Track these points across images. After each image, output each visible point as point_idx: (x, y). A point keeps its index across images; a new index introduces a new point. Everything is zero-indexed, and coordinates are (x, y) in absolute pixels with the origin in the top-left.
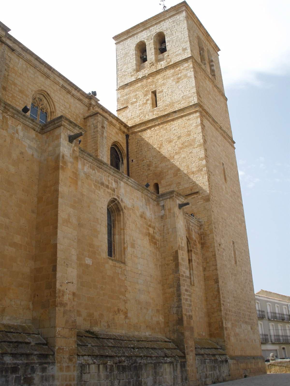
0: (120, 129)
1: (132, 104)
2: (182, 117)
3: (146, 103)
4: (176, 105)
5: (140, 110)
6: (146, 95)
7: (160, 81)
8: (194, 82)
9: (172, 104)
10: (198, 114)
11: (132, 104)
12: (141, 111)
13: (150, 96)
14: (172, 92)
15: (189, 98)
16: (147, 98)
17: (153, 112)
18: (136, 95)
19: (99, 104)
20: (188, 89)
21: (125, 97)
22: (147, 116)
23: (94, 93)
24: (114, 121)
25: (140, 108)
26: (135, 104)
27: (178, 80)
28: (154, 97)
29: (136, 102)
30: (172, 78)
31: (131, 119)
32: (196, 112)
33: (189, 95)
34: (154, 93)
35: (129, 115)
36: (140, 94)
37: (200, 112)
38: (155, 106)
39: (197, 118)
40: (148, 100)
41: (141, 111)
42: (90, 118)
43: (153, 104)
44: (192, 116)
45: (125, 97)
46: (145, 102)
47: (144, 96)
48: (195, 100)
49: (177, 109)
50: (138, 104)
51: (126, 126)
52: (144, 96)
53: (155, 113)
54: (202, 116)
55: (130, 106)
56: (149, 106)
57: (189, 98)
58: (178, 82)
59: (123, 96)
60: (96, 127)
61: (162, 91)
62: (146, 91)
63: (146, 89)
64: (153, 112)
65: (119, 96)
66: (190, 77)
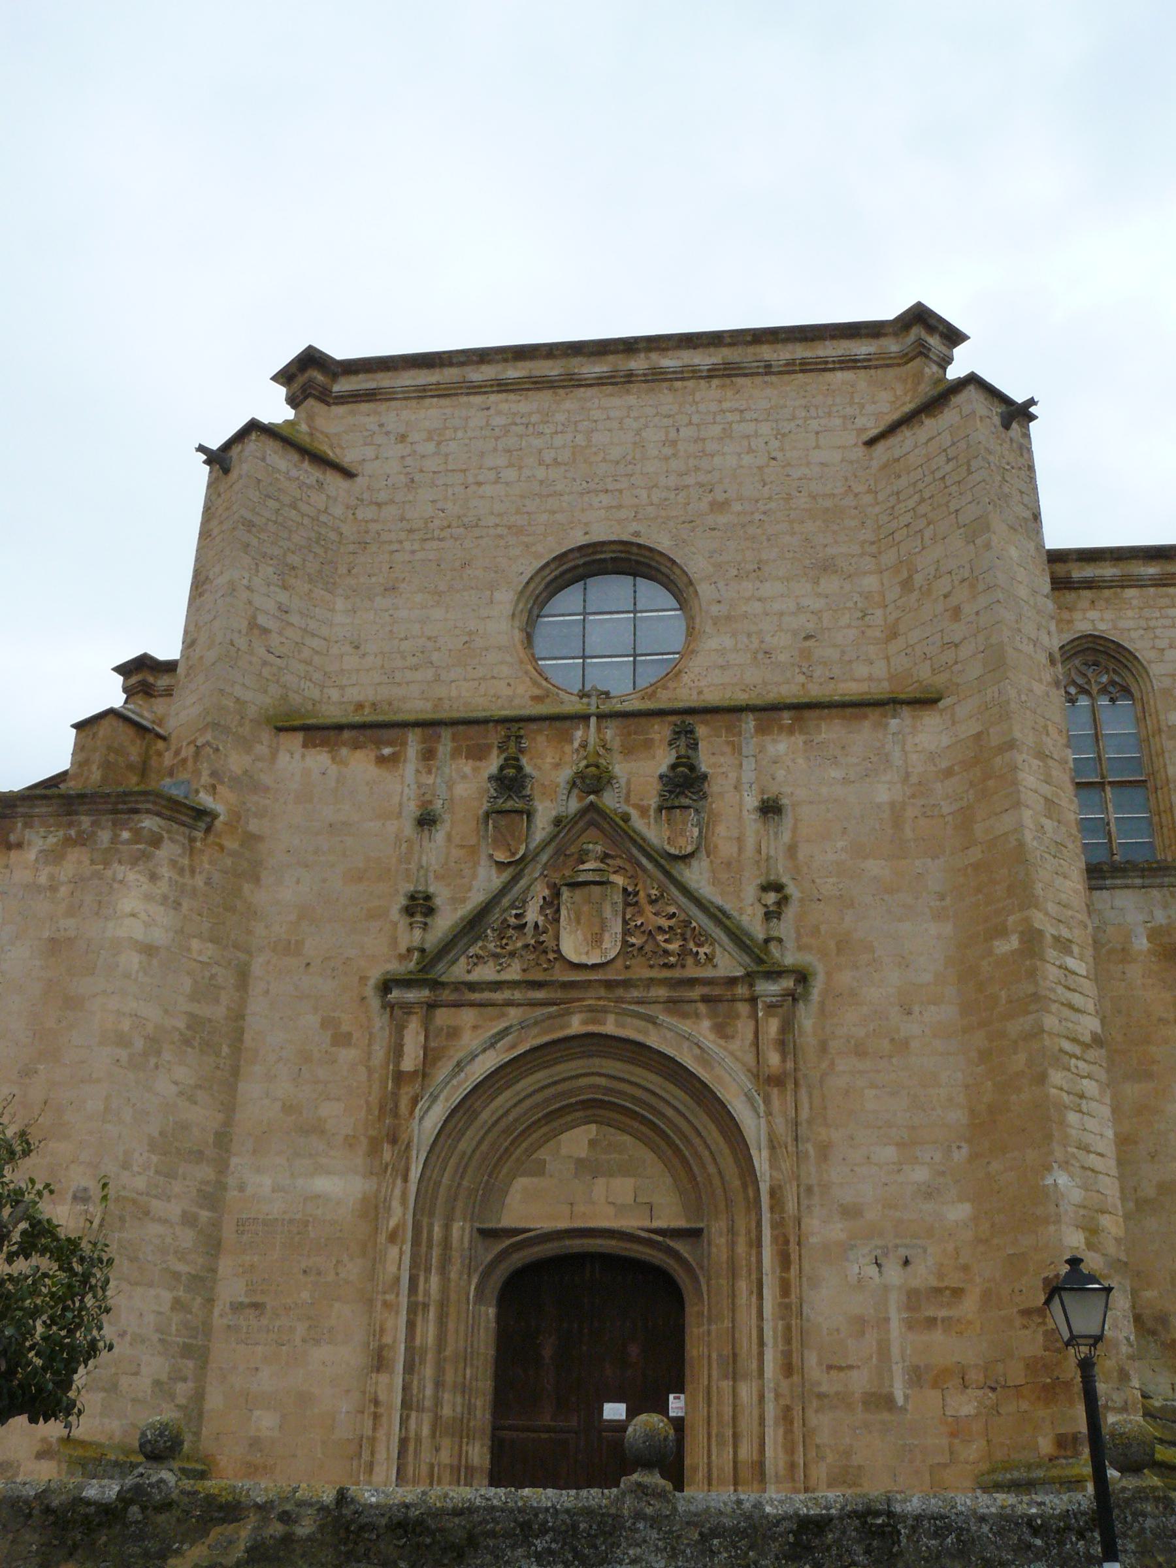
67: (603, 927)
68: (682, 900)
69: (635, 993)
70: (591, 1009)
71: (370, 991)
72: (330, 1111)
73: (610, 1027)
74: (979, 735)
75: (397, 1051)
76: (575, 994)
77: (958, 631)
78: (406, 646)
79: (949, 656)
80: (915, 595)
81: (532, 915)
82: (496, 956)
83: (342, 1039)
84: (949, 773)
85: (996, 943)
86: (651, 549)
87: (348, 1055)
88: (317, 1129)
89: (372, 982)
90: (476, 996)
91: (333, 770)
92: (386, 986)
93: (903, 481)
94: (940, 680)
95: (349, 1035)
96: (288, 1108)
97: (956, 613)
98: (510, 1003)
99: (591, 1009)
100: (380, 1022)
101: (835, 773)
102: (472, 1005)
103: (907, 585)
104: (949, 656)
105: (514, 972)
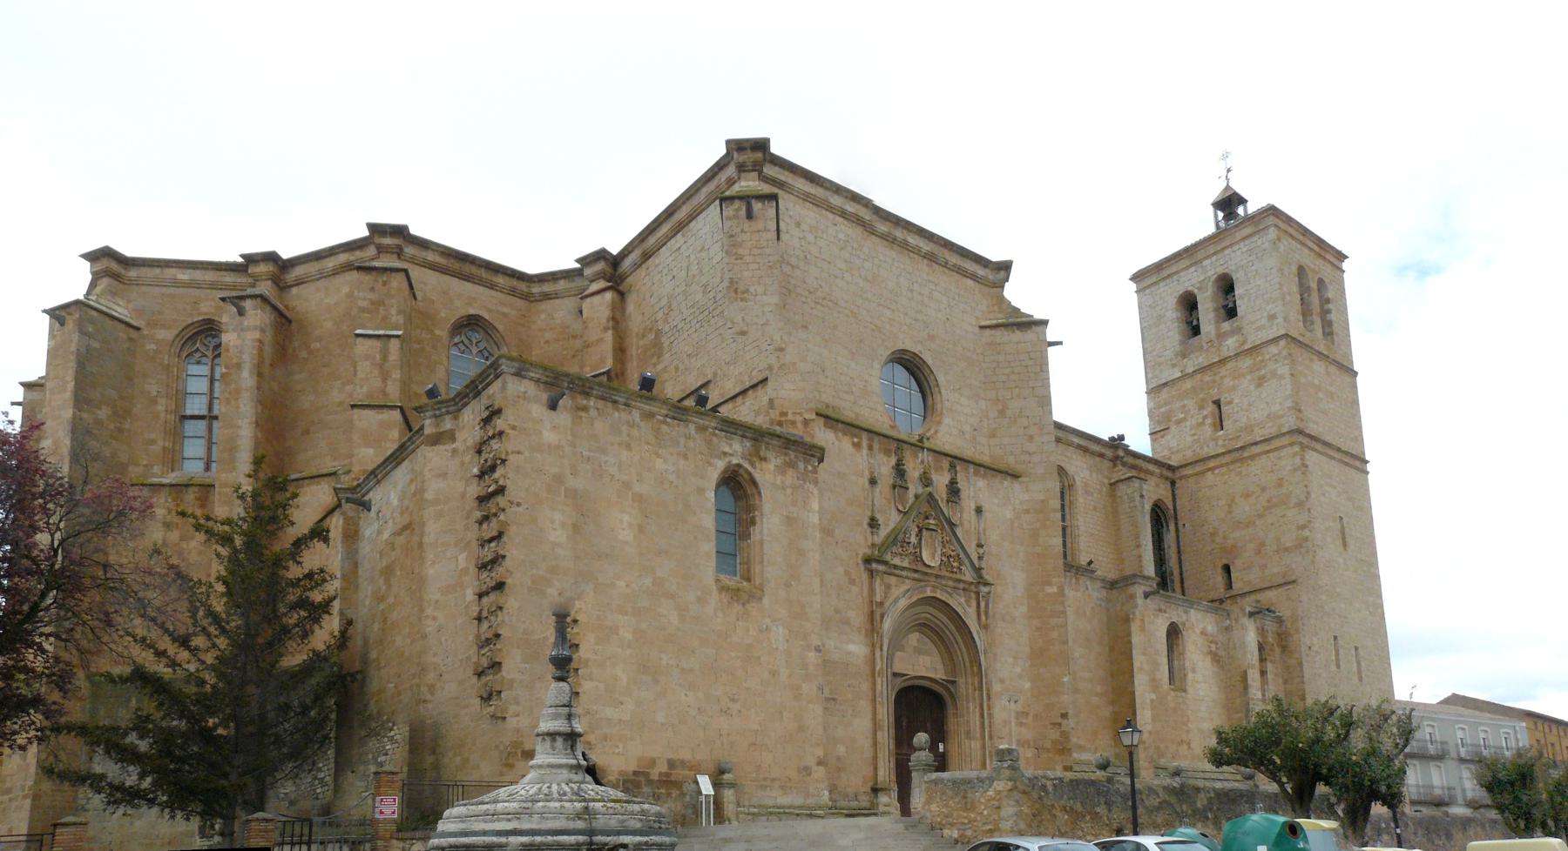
0: (1161, 476)
1: (1179, 422)
2: (1268, 452)
3: (1202, 424)
4: (1256, 429)
5: (1194, 435)
6: (1201, 408)
7: (1228, 382)
8: (1289, 387)
9: (1249, 429)
10: (1296, 448)
11: (1179, 422)
12: (1196, 437)
13: (1211, 408)
14: (1250, 404)
15: (1282, 416)
16: (1205, 413)
17: (1216, 439)
18: (1184, 406)
19: (1131, 451)
20: (1278, 401)
21: (1163, 410)
22: (1206, 449)
23: (1122, 438)
24: (1151, 467)
25: (1193, 432)
26: (1183, 424)
27: (1261, 382)
28: (1217, 411)
29: (1185, 419)
30: (1249, 377)
31: (1177, 452)
32: (1292, 444)
33: (1281, 413)
34: (1217, 403)
35: (1173, 444)
36: (1190, 403)
37: (1301, 443)
38: (1219, 428)
39: (1295, 454)
40: (1205, 417)
41: (1196, 437)
42: (1120, 484)
43: (1214, 425)
44: (1283, 452)
45: (1163, 410)
46: (1201, 420)
47: (1200, 409)
48: (1290, 422)
49: (1258, 439)
50: (1188, 423)
51: (1170, 468)
52: (1200, 409)
53: (1220, 442)
54: (1303, 447)
55: (1173, 428)
56: (1208, 430)
57: (1282, 416)
58: (1259, 385)
59: (1160, 407)
60: (1132, 500)
61: (1230, 402)
62: (1203, 400)
63: (1201, 396)
64: (1216, 439)
65: (1152, 405)
66: (1282, 377)
67: (935, 551)
68: (956, 544)
69: (944, 582)
70: (933, 586)
71: (860, 562)
72: (852, 614)
73: (938, 596)
74: (1043, 501)
75: (872, 590)
76: (926, 578)
77: (1032, 448)
78: (842, 378)
79: (1026, 458)
80: (1006, 421)
81: (913, 540)
82: (901, 555)
83: (852, 582)
84: (1027, 511)
85: (1046, 587)
86: (924, 362)
87: (855, 589)
88: (847, 622)
89: (860, 556)
90: (896, 572)
91: (837, 443)
92: (868, 561)
93: (1001, 358)
94: (1020, 468)
95: (854, 580)
96: (837, 611)
97: (1031, 438)
98: (907, 578)
99: (933, 586)
100: (865, 576)
101: (996, 501)
102: (895, 575)
103: (1002, 413)
104: (1026, 458)
105: (905, 564)
